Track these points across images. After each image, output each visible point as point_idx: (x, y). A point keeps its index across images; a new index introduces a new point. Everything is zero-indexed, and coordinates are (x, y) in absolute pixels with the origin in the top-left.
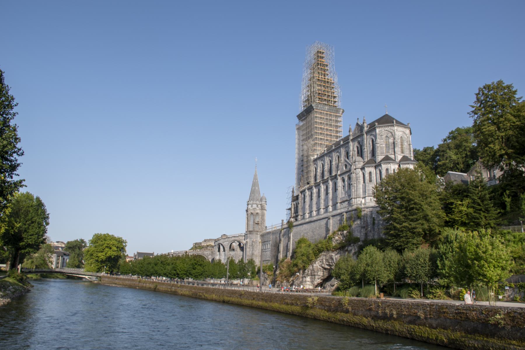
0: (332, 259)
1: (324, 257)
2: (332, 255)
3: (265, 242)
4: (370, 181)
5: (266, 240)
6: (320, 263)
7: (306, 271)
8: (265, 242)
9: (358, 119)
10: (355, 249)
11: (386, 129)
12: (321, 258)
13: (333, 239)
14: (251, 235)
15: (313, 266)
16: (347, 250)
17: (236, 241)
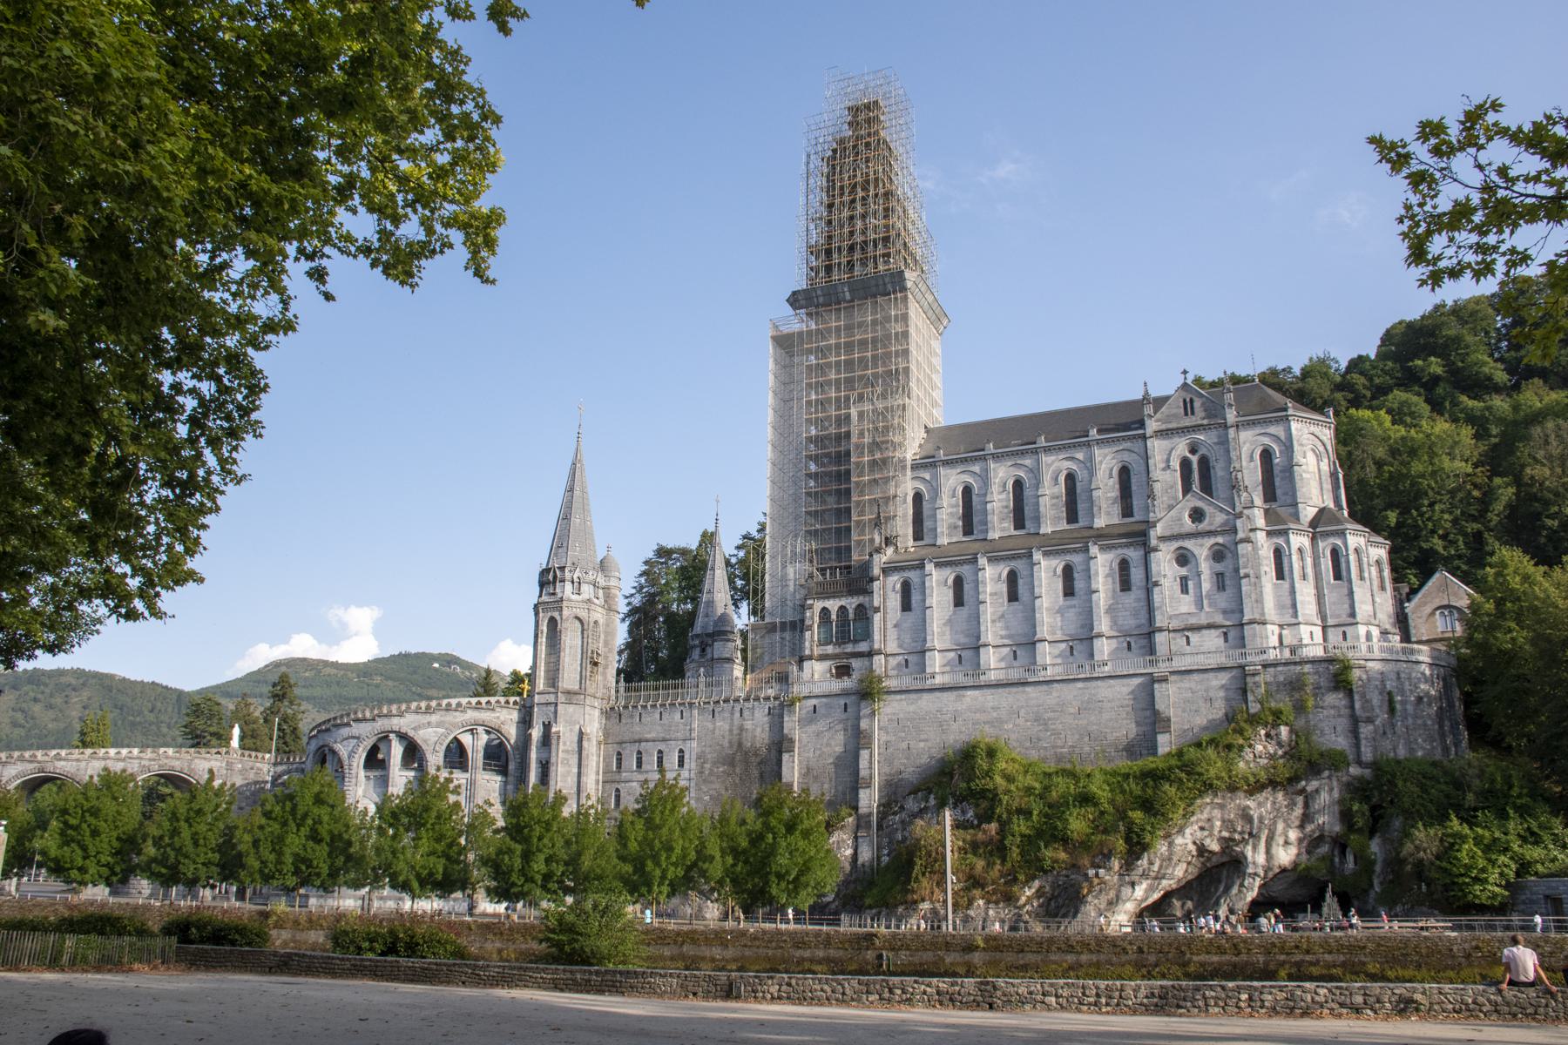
0: (1248, 819)
1: (1217, 813)
2: (1249, 807)
3: (640, 741)
4: (1304, 577)
5: (648, 736)
6: (1199, 834)
7: (1143, 862)
8: (640, 741)
9: (1185, 372)
10: (1331, 790)
11: (1313, 429)
12: (1205, 816)
13: (1247, 750)
14: (571, 708)
15: (1171, 844)
16: (1303, 791)
17: (480, 729)
